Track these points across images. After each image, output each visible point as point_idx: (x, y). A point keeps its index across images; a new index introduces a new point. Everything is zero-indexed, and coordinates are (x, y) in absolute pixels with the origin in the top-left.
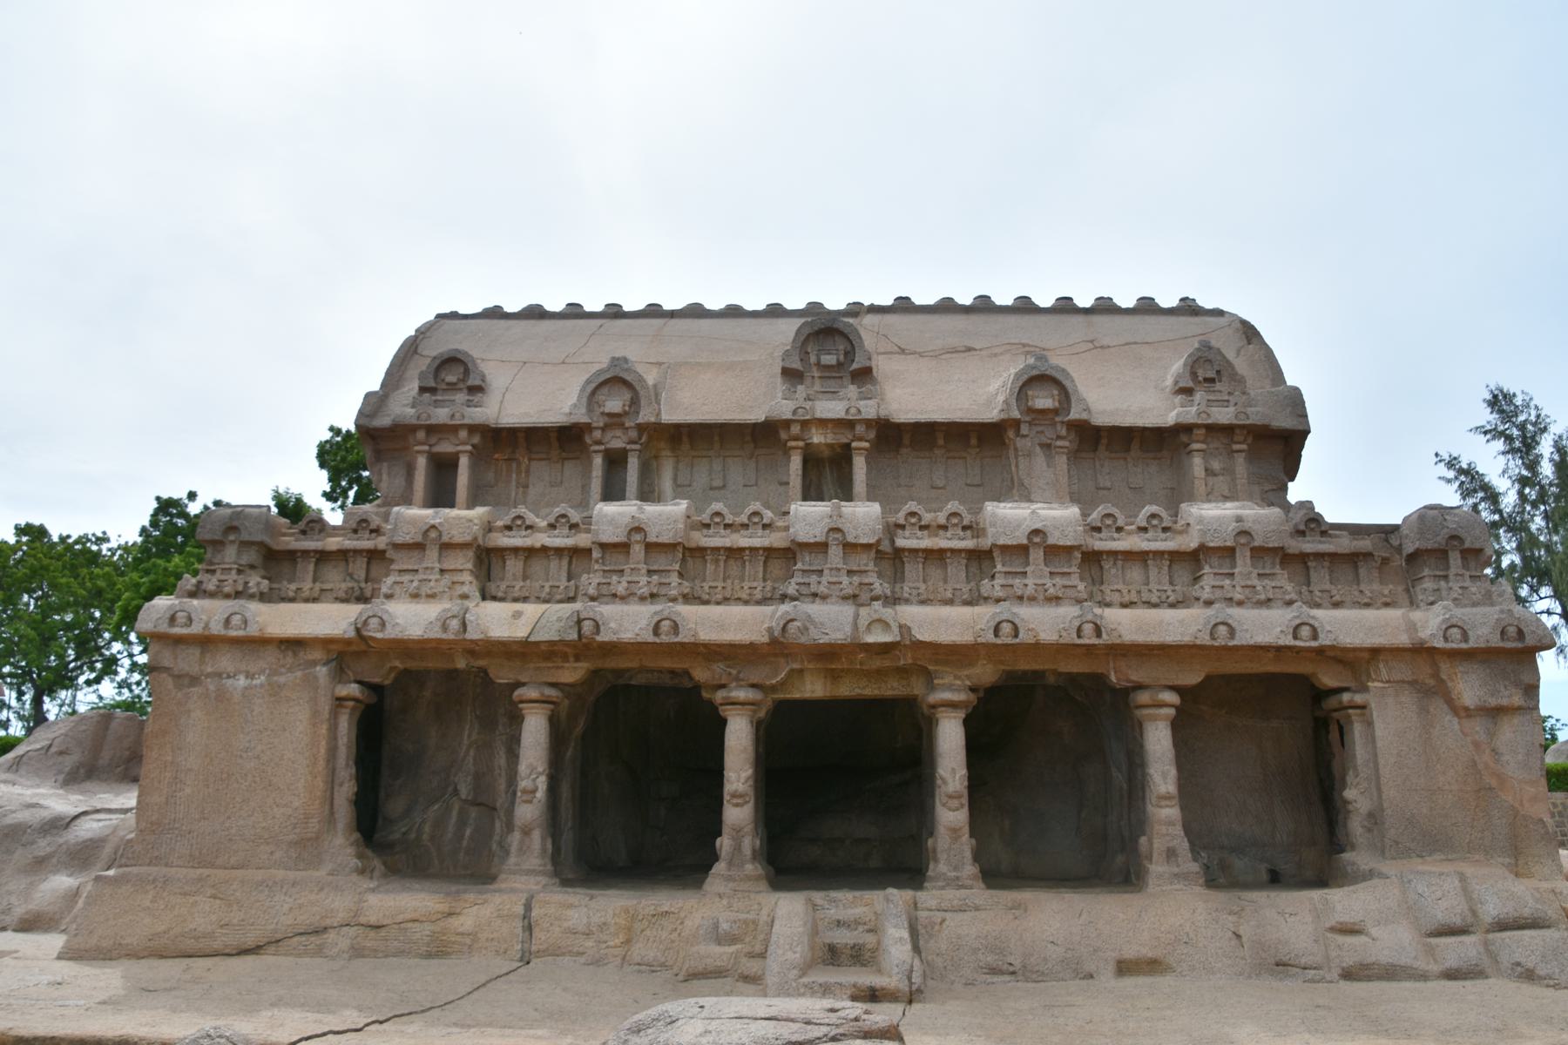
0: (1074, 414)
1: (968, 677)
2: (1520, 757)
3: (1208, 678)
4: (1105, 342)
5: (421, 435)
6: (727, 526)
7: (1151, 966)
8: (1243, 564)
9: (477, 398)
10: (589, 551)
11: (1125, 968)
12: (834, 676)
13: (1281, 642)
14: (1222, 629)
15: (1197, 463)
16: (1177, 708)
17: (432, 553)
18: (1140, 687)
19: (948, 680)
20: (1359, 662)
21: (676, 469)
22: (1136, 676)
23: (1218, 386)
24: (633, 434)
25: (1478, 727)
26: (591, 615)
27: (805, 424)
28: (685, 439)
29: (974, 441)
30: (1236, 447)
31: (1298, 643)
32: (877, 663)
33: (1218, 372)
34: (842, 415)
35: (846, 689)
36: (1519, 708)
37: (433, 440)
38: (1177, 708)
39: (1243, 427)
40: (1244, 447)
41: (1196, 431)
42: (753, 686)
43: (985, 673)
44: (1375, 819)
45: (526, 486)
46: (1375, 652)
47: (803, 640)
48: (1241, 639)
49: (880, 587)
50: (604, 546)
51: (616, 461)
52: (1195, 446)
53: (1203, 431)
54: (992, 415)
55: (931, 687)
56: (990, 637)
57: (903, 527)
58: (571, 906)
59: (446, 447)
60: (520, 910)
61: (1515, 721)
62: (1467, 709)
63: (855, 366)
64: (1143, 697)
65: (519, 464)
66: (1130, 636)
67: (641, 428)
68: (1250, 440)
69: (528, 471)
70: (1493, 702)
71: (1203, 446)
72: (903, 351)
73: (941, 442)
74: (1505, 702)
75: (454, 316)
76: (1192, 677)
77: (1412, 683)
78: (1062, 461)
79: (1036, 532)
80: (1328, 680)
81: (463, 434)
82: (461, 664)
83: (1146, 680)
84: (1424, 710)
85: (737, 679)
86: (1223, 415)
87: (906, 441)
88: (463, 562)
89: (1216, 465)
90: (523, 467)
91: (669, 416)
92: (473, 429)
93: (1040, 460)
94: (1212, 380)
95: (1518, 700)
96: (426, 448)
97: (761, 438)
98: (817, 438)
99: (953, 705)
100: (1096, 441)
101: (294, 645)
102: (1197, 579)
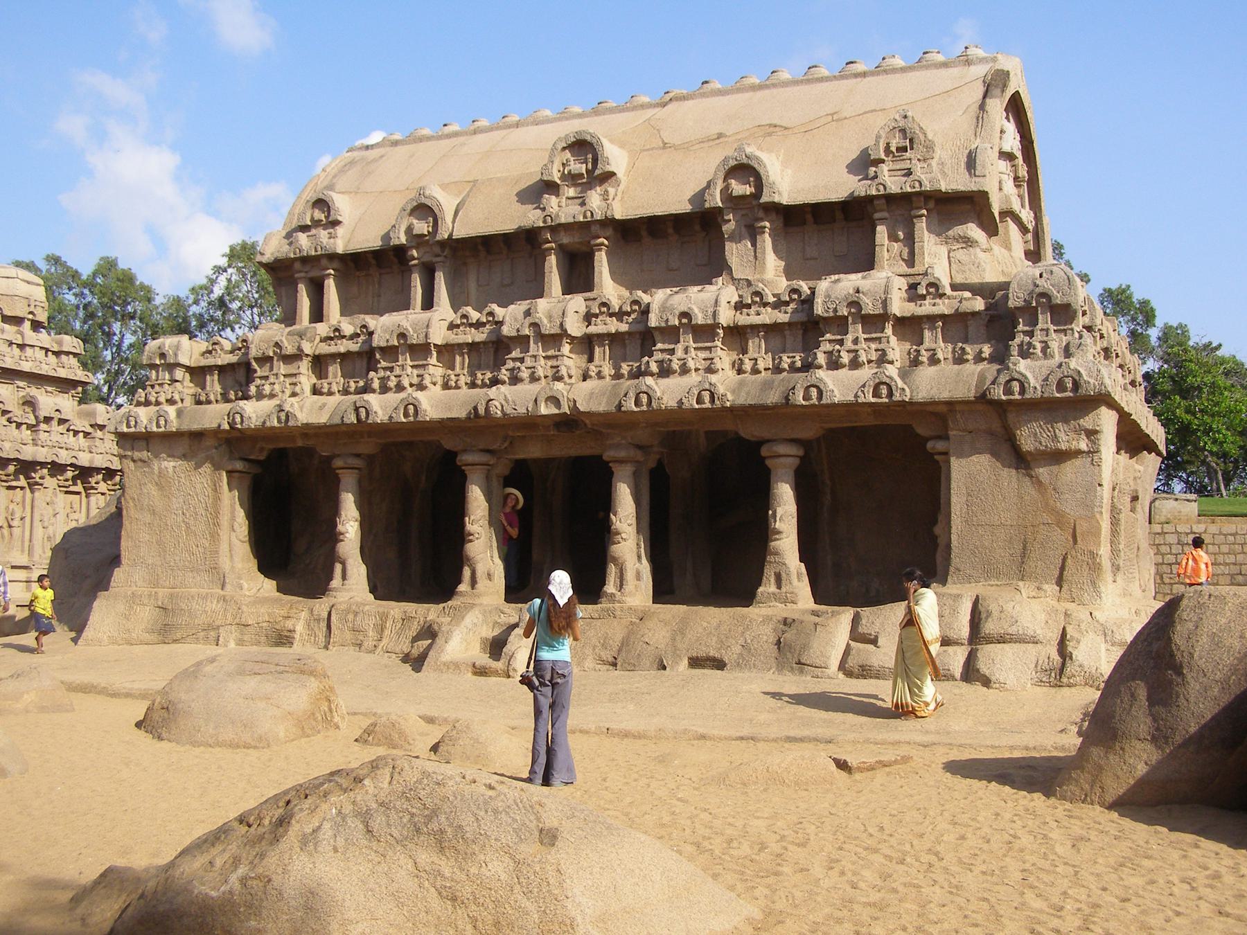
0: (765, 199)
2: (1078, 495)
4: (845, 114)
5: (297, 266)
6: (471, 325)
7: (719, 664)
8: (856, 331)
11: (695, 663)
14: (814, 392)
15: (882, 231)
16: (801, 458)
18: (760, 443)
19: (617, 440)
20: (941, 414)
23: (908, 155)
24: (437, 250)
26: (363, 404)
27: (556, 229)
28: (480, 247)
29: (697, 227)
30: (914, 212)
31: (880, 400)
33: (911, 141)
37: (307, 268)
38: (801, 458)
41: (876, 202)
42: (482, 451)
44: (948, 546)
46: (950, 404)
51: (429, 274)
52: (877, 215)
53: (883, 201)
57: (596, 316)
59: (315, 273)
60: (325, 615)
63: (597, 172)
68: (931, 205)
71: (885, 214)
72: (665, 146)
73: (670, 231)
76: (809, 432)
80: (922, 431)
82: (300, 443)
87: (644, 233)
94: (904, 149)
96: (302, 275)
98: (566, 240)
100: (795, 219)
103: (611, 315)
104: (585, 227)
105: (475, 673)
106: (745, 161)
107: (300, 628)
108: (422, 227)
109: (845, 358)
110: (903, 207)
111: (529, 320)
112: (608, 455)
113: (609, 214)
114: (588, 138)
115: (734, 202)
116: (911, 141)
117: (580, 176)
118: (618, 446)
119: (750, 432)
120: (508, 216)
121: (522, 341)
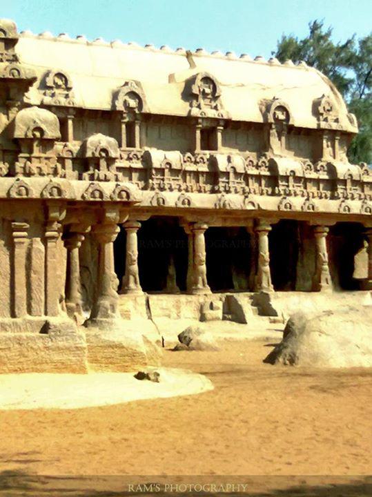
0: (291, 123)
1: (270, 221)
3: (337, 223)
8: (349, 185)
12: (225, 220)
21: (147, 129)
22: (319, 222)
27: (203, 118)
33: (331, 108)
34: (217, 116)
35: (228, 224)
43: (275, 221)
45: (86, 132)
58: (162, 300)
60: (145, 302)
64: (319, 229)
65: (83, 122)
66: (321, 209)
69: (87, 125)
76: (333, 223)
79: (292, 171)
81: (71, 111)
85: (201, 220)
86: (334, 126)
90: (85, 124)
91: (154, 111)
97: (187, 123)
102: (336, 189)
103: (253, 166)
104: (216, 121)
105: (271, 322)
106: (283, 105)
107: (133, 310)
108: (133, 103)
109: (350, 196)
110: (333, 133)
111: (231, 165)
113: (230, 117)
114: (211, 77)
115: (276, 119)
116: (331, 108)
117: (208, 94)
118: (264, 224)
120: (179, 108)
121: (227, 174)
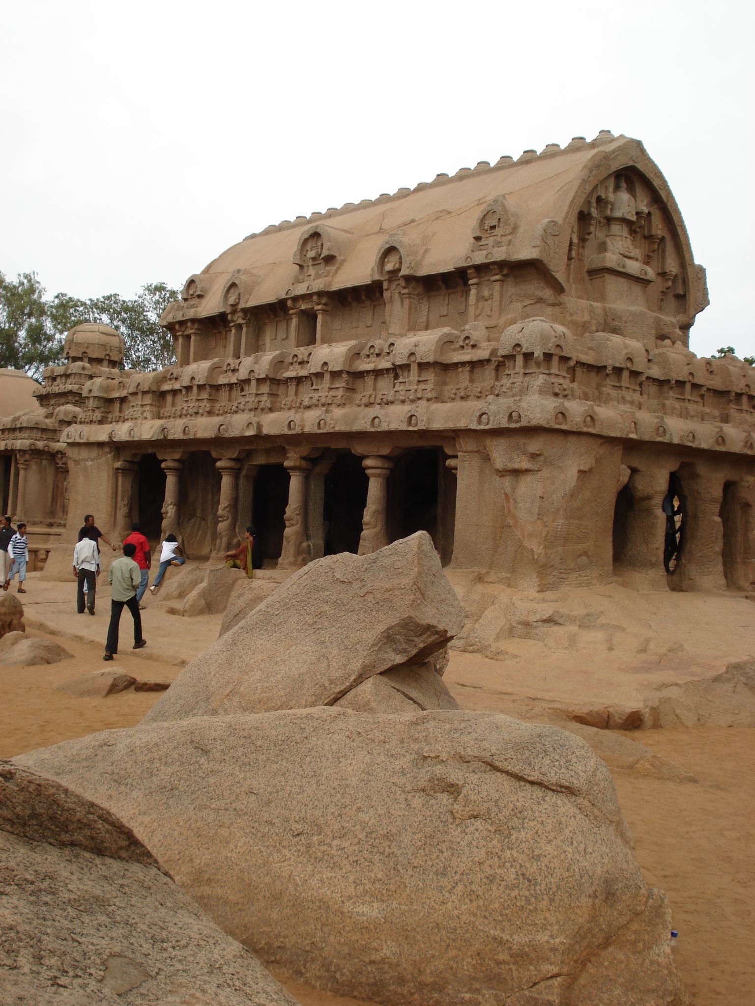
5: (177, 327)
9: (332, 268)
10: (180, 390)
13: (400, 429)
17: (140, 396)
25: (507, 481)
27: (295, 299)
32: (268, 446)
36: (527, 471)
39: (494, 263)
40: (497, 277)
47: (226, 435)
48: (384, 427)
49: (266, 401)
50: (184, 387)
54: (368, 281)
55: (287, 458)
56: (286, 431)
61: (528, 479)
62: (498, 470)
67: (245, 311)
70: (511, 466)
74: (516, 466)
75: (253, 236)
77: (478, 452)
78: (406, 302)
79: (325, 364)
83: (365, 453)
84: (482, 471)
88: (148, 400)
89: (486, 293)
92: (193, 321)
93: (397, 304)
95: (525, 464)
99: (294, 468)
101: (100, 445)
112: (286, 464)
119: (359, 449)
